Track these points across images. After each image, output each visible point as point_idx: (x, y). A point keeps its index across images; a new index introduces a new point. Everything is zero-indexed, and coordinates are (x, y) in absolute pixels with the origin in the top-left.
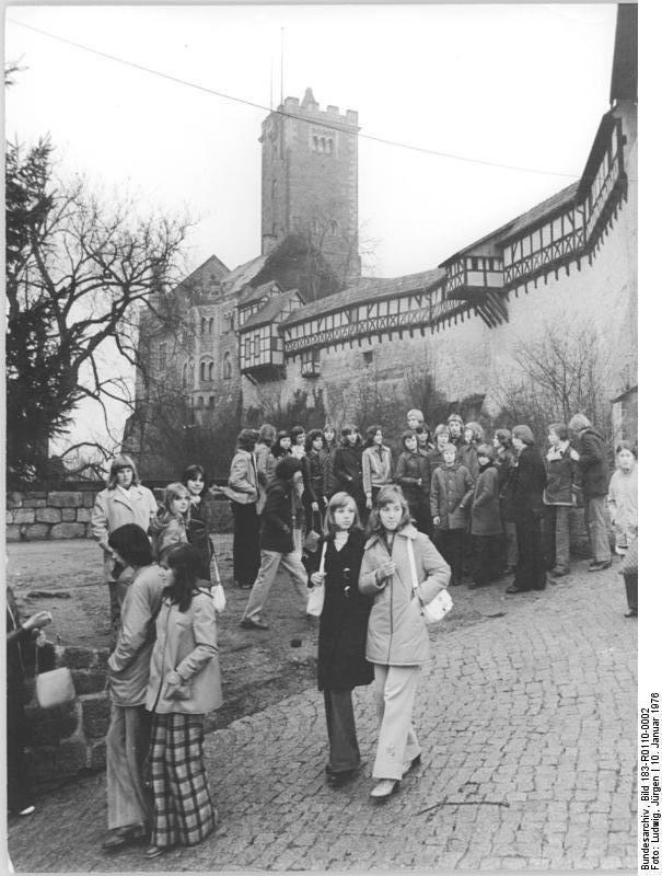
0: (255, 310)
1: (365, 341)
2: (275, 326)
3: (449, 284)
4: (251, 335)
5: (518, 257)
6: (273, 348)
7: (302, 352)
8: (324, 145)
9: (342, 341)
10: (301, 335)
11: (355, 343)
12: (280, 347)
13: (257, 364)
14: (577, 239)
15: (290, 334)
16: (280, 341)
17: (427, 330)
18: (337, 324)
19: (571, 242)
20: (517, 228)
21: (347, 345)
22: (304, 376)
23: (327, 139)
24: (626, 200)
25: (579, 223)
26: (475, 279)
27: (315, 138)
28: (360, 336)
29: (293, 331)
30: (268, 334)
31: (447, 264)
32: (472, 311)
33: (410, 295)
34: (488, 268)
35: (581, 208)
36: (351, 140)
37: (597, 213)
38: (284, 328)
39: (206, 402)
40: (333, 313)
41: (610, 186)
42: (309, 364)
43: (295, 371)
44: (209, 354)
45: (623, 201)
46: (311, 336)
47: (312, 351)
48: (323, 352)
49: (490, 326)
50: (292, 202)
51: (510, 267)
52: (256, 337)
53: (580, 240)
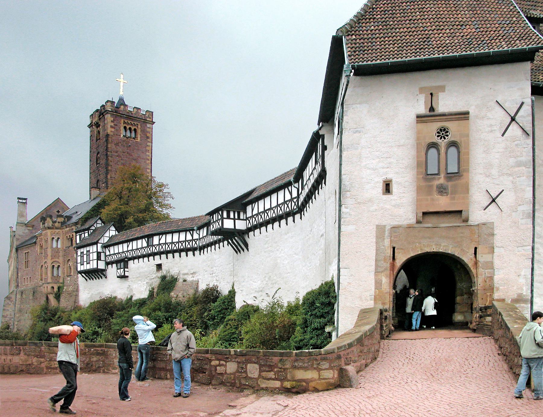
0: (86, 235)
1: (157, 257)
3: (212, 226)
4: (85, 250)
5: (255, 212)
6: (99, 258)
7: (117, 262)
8: (131, 132)
9: (143, 256)
10: (116, 251)
11: (151, 258)
12: (103, 258)
13: (88, 268)
14: (293, 204)
15: (109, 251)
16: (103, 255)
17: (197, 253)
18: (140, 246)
19: (290, 205)
20: (255, 195)
21: (146, 259)
22: (118, 277)
24: (325, 183)
25: (295, 194)
26: (228, 224)
27: (125, 128)
28: (154, 254)
29: (112, 248)
30: (95, 250)
31: (211, 214)
32: (226, 242)
33: (186, 231)
34: (236, 217)
35: (296, 185)
36: (148, 130)
37: (306, 190)
38: (106, 246)
39: (56, 289)
40: (137, 239)
41: (316, 175)
42: (122, 270)
43: (112, 271)
44: (57, 260)
45: (323, 185)
46: (123, 252)
47: (123, 262)
48: (131, 263)
49: (237, 253)
50: (110, 168)
51: (250, 217)
52: (87, 251)
53: (295, 204)
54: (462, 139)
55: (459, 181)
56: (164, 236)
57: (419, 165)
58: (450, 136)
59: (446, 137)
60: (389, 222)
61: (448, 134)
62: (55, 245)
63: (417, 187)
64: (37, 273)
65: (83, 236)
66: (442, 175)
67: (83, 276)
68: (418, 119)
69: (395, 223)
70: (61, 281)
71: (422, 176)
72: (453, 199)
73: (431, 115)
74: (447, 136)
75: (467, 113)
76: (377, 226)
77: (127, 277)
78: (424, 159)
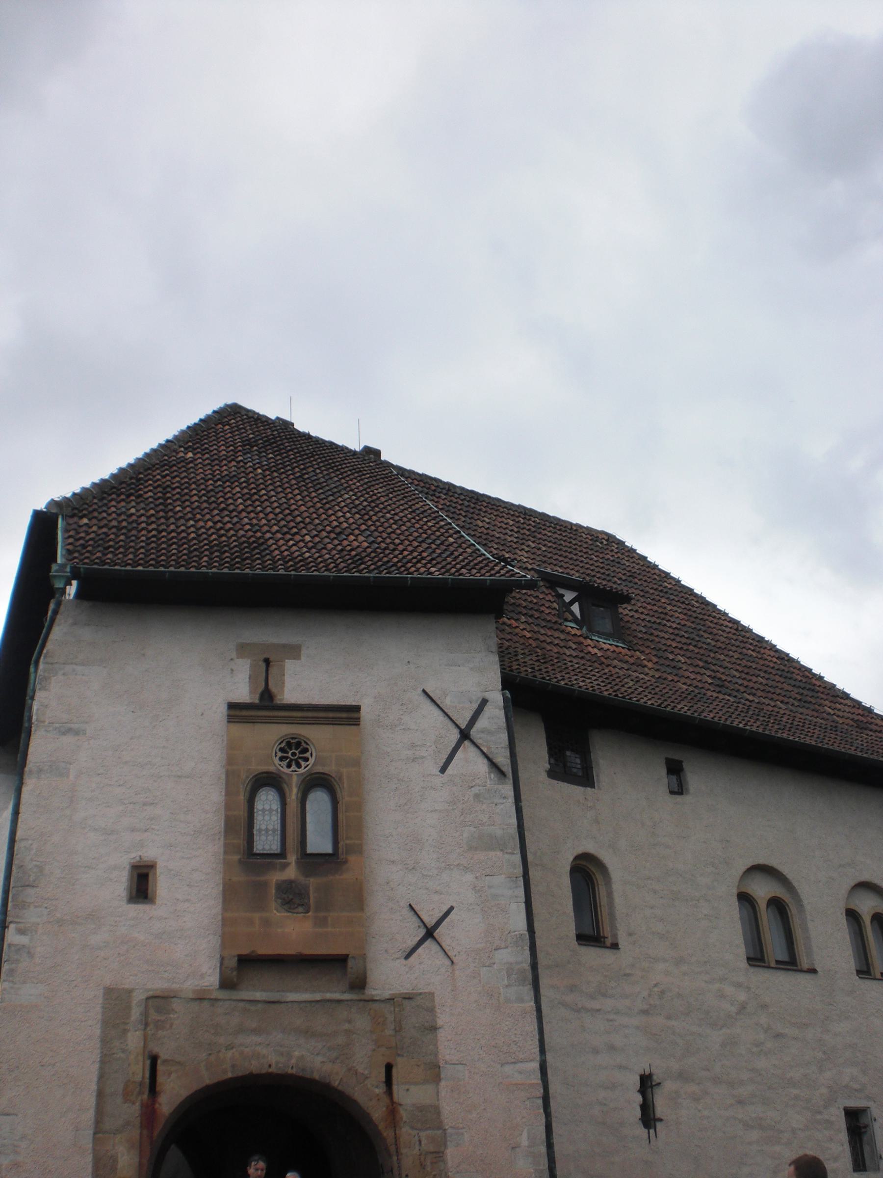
54: (344, 771)
55: (337, 877)
57: (230, 827)
58: (312, 761)
59: (303, 763)
60: (142, 981)
61: (307, 755)
63: (225, 885)
66: (292, 858)
68: (233, 712)
69: (159, 984)
71: (236, 857)
72: (322, 922)
73: (263, 707)
74: (306, 760)
75: (357, 709)
76: (109, 992)
78: (242, 812)
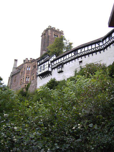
2: (50, 61)
4: (42, 65)
6: (49, 67)
8: (56, 36)
9: (72, 60)
11: (76, 60)
12: (51, 66)
15: (54, 63)
16: (51, 65)
17: (102, 52)
21: (73, 61)
23: (57, 35)
27: (54, 35)
28: (78, 58)
30: (48, 63)
43: (55, 72)
44: (28, 75)
56: (83, 49)
62: (28, 69)
64: (19, 83)
65: (41, 62)
67: (40, 77)
70: (29, 83)
77: (63, 71)
